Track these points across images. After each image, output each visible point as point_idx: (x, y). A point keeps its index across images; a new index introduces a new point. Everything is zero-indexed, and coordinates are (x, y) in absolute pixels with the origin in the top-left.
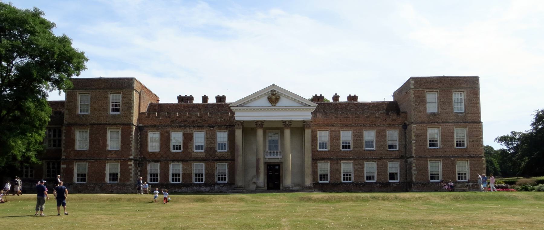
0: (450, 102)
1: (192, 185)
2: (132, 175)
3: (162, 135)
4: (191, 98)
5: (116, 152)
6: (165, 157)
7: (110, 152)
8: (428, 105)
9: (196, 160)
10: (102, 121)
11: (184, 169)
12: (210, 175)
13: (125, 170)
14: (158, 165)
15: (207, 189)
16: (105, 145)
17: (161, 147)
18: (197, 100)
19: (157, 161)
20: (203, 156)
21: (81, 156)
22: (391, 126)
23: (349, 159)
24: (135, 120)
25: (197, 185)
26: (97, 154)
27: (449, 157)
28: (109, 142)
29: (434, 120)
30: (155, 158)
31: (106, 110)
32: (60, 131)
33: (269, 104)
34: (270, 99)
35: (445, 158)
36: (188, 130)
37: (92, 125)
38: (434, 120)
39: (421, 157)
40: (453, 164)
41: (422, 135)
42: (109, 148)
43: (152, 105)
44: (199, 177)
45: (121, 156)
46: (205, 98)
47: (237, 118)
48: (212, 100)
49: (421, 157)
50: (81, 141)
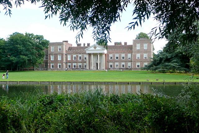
0: (143, 46)
1: (78, 69)
2: (64, 66)
3: (71, 56)
4: (81, 44)
5: (60, 61)
6: (71, 62)
7: (59, 61)
8: (137, 47)
9: (79, 62)
10: (57, 53)
11: (76, 65)
12: (83, 66)
13: (63, 65)
14: (70, 63)
15: (82, 70)
16: (58, 59)
17: (71, 59)
18: (82, 45)
19: (70, 63)
20: (81, 61)
21: (52, 62)
22: (129, 53)
23: (118, 62)
24: (64, 52)
25: (79, 69)
26: (56, 61)
27: (141, 62)
28: (58, 58)
29: (138, 51)
30: (69, 62)
31: (58, 50)
32: (47, 55)
33: (94, 49)
34: (94, 48)
35: (141, 62)
36: (77, 55)
37: (55, 54)
38: (138, 51)
39: (134, 62)
40: (143, 63)
41: (135, 56)
42: (58, 60)
43: (69, 47)
44: (80, 66)
45: (62, 61)
46: (84, 44)
47: (87, 53)
48: (86, 45)
49: (134, 62)
50: (52, 58)
